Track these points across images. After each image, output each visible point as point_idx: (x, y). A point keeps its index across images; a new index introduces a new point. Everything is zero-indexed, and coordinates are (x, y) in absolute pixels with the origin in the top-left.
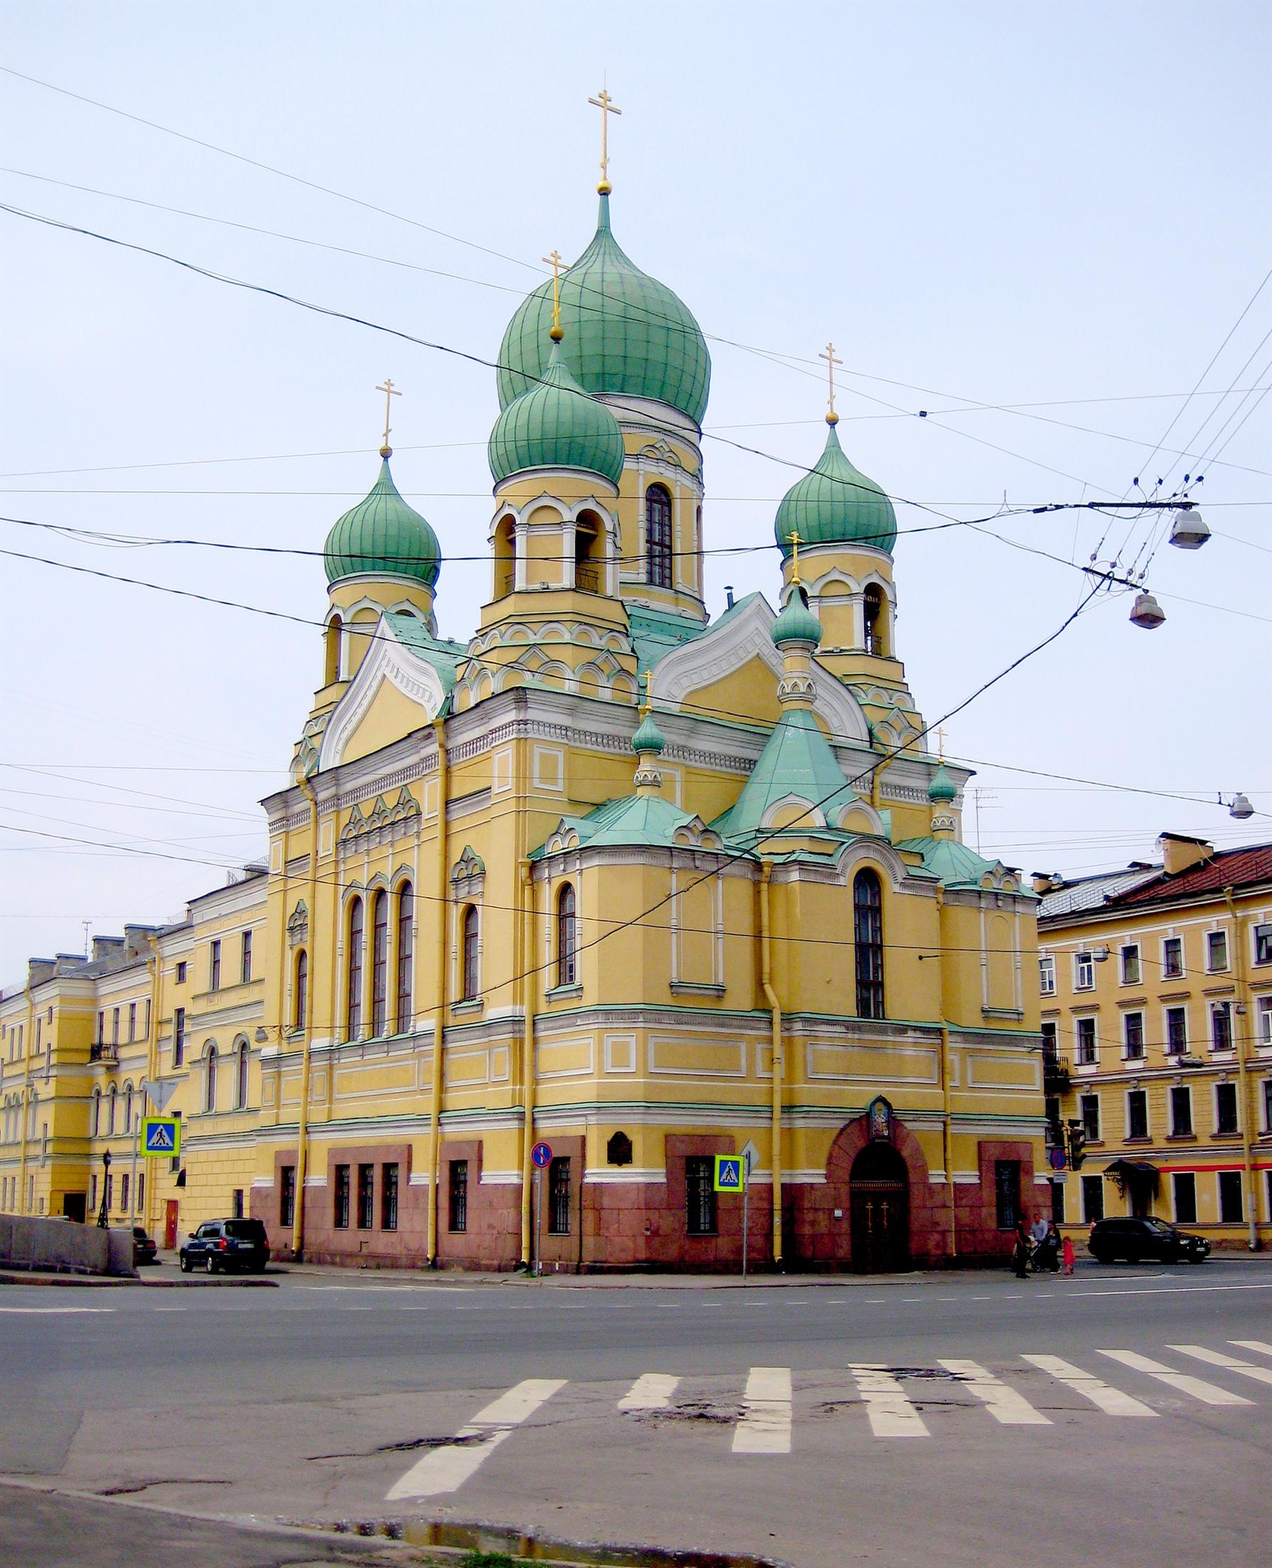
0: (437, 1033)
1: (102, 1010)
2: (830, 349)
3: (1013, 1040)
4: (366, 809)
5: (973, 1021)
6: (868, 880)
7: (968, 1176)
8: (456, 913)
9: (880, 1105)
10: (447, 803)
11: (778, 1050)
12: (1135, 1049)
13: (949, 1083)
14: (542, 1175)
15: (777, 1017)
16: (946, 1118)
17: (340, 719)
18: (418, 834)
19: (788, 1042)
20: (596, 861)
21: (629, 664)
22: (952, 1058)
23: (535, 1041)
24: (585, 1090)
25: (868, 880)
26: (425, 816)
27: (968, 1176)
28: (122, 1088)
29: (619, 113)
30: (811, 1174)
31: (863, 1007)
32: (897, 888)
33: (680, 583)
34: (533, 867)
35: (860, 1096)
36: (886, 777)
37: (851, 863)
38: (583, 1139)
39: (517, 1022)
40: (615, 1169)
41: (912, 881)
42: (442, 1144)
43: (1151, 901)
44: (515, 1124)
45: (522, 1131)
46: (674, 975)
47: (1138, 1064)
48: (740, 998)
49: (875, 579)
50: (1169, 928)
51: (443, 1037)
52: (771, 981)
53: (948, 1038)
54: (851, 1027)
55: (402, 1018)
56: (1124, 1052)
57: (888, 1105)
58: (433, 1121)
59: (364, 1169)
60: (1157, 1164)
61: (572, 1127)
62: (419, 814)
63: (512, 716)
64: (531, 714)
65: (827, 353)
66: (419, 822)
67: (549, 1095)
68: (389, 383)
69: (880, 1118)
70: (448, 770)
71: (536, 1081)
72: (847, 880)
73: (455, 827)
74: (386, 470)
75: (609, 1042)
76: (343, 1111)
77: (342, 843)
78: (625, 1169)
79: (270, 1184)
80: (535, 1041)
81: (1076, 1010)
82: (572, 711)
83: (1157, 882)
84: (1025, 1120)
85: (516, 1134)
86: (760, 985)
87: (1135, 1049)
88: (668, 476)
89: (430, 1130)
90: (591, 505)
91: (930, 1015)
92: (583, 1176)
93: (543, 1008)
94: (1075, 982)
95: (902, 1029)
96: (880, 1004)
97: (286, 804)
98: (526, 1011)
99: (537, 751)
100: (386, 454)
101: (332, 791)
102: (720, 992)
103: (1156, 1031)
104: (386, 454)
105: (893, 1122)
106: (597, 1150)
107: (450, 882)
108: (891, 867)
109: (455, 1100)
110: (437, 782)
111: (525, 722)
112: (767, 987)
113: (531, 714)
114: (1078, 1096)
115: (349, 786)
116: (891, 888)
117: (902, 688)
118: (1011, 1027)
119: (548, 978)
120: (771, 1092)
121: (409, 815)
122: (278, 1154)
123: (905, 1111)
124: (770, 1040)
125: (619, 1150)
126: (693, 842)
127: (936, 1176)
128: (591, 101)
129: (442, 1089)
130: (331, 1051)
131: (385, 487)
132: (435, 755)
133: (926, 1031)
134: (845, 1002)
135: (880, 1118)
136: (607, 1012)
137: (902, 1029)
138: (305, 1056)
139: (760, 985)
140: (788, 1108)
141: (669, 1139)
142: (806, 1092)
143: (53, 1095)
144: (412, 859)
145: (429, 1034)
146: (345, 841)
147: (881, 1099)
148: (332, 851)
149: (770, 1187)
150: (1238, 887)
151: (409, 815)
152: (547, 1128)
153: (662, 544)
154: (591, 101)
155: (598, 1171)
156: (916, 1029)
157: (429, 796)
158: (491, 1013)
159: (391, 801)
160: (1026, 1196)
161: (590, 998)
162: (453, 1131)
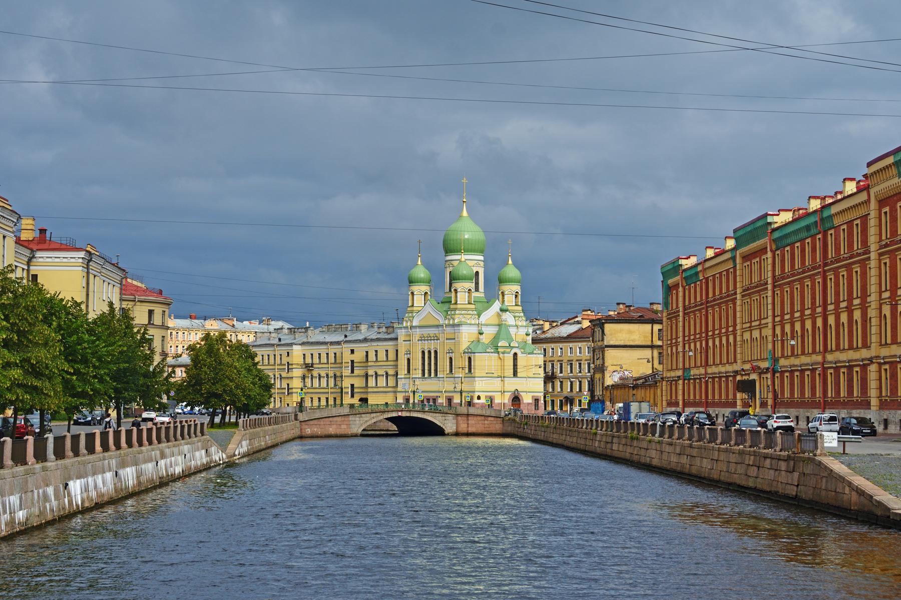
6: (515, 354)
25: (515, 354)
28: (315, 373)
30: (506, 401)
31: (514, 376)
43: (575, 338)
47: (572, 375)
55: (436, 375)
69: (516, 392)
96: (517, 374)
116: (519, 355)
135: (516, 392)
155: (476, 401)
160: (539, 405)
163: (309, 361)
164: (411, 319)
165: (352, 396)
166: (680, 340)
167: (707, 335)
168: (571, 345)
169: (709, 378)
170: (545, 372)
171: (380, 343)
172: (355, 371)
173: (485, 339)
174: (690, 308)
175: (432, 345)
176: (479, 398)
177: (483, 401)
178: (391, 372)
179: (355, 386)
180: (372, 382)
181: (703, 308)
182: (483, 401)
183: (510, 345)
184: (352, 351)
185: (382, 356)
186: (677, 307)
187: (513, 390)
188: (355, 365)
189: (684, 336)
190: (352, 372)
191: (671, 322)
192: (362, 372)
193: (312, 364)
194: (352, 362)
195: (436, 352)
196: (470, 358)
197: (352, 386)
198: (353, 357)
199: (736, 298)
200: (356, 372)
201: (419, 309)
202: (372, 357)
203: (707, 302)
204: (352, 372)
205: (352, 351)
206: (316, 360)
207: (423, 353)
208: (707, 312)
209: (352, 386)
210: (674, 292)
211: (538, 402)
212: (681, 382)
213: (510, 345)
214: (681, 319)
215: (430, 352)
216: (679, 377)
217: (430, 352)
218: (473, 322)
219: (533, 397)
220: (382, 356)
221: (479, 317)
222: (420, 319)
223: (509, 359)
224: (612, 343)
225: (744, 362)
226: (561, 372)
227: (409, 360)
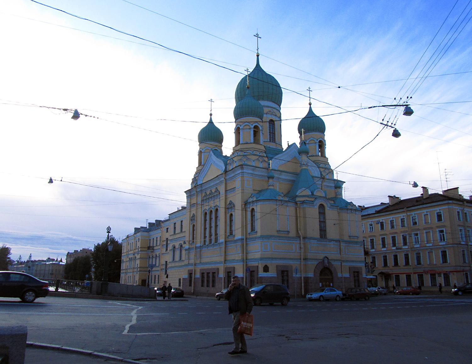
0: (224, 242)
2: (309, 88)
3: (356, 243)
5: (346, 238)
6: (322, 206)
7: (347, 275)
8: (228, 216)
9: (326, 258)
10: (226, 191)
11: (302, 246)
12: (384, 246)
13: (342, 253)
14: (248, 274)
15: (302, 238)
16: (342, 261)
17: (202, 173)
18: (220, 199)
19: (304, 244)
20: (260, 203)
23: (246, 244)
24: (258, 255)
25: (322, 206)
26: (221, 194)
27: (347, 275)
29: (261, 38)
30: (311, 275)
32: (328, 208)
34: (245, 205)
35: (321, 256)
36: (324, 184)
37: (318, 202)
38: (258, 266)
39: (242, 239)
40: (265, 273)
42: (226, 268)
44: (242, 263)
45: (244, 265)
46: (278, 229)
47: (385, 249)
48: (293, 234)
49: (321, 139)
50: (391, 217)
51: (226, 243)
52: (300, 230)
53: (341, 243)
56: (381, 246)
57: (327, 258)
58: (223, 263)
59: (208, 273)
60: (390, 273)
61: (255, 264)
63: (240, 171)
64: (244, 171)
65: (309, 89)
66: (220, 195)
67: (250, 256)
68: (211, 100)
69: (326, 261)
70: (226, 184)
72: (317, 207)
73: (228, 196)
74: (211, 118)
76: (204, 260)
77: (202, 201)
78: (267, 273)
79: (187, 277)
80: (246, 244)
81: (370, 236)
82: (253, 170)
83: (388, 207)
84: (360, 262)
85: (242, 265)
86: (297, 231)
87: (384, 246)
88: (274, 118)
89: (222, 265)
90: (256, 124)
91: (337, 237)
92: (258, 275)
93: (248, 237)
94: (369, 230)
96: (325, 235)
97: (190, 193)
98: (244, 237)
100: (211, 115)
101: (200, 189)
103: (389, 241)
104: (211, 115)
105: (329, 263)
106: (261, 269)
107: (227, 209)
108: (327, 204)
109: (230, 258)
111: (243, 172)
112: (299, 231)
113: (244, 171)
115: (204, 188)
116: (327, 209)
120: (301, 255)
122: (189, 270)
123: (331, 260)
124: (300, 243)
125: (266, 269)
127: (340, 275)
128: (254, 36)
129: (225, 255)
131: (211, 122)
132: (223, 181)
133: (336, 241)
134: (317, 234)
135: (326, 261)
136: (262, 237)
137: (331, 240)
138: (195, 248)
139: (297, 231)
140: (305, 259)
141: (277, 266)
142: (309, 256)
145: (222, 243)
146: (203, 200)
147: (326, 257)
148: (200, 202)
149: (301, 277)
150: (407, 208)
153: (272, 133)
154: (254, 36)
155: (262, 274)
156: (334, 241)
157: (222, 189)
158: (236, 238)
159: (213, 191)
161: (259, 234)
162: (229, 265)
173: (279, 186)
175: (212, 204)
176: (266, 269)
177: (272, 273)
182: (272, 273)
183: (313, 194)
187: (321, 258)
193: (153, 247)
211: (358, 276)
213: (313, 194)
218: (261, 165)
219: (350, 268)
223: (313, 212)
226: (373, 248)
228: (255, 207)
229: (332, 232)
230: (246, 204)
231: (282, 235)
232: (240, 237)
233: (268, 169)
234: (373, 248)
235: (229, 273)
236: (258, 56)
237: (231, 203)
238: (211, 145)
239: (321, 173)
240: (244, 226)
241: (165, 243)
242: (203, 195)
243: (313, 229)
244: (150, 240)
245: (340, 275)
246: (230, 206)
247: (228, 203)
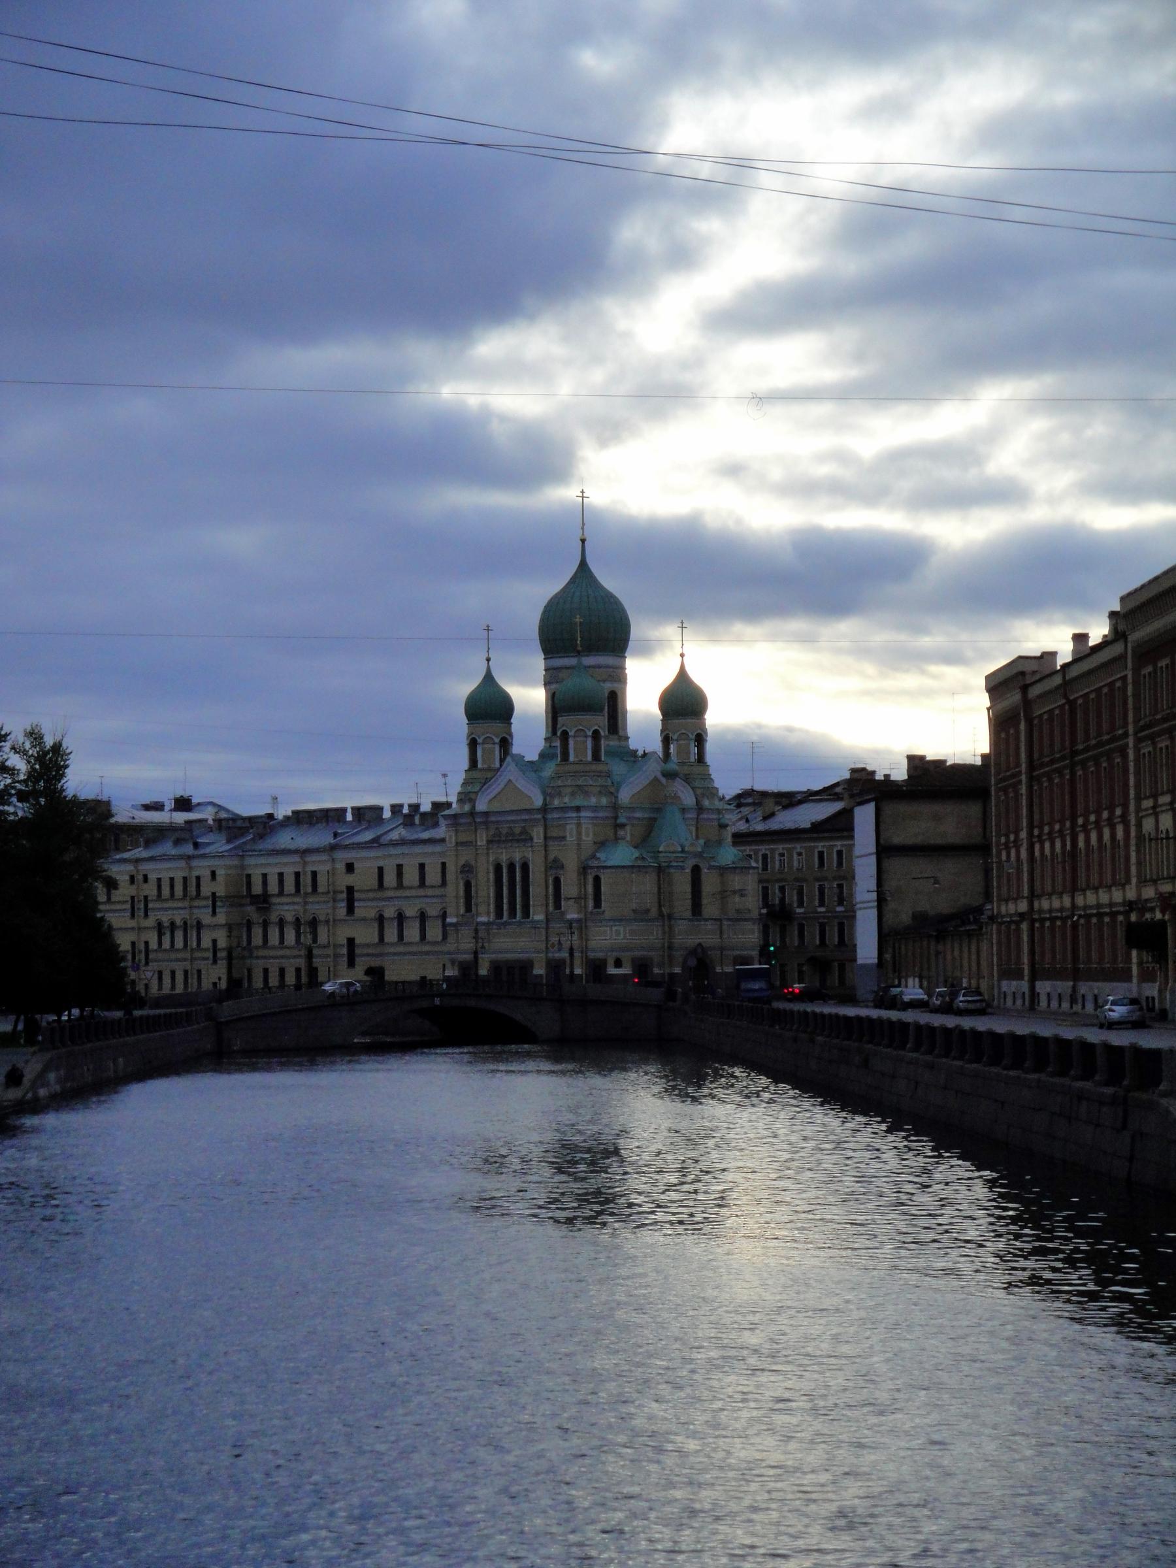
1: (250, 872)
3: (746, 920)
4: (504, 831)
6: (696, 870)
11: (667, 929)
16: (722, 949)
21: (612, 790)
22: (725, 927)
25: (696, 870)
26: (535, 841)
30: (677, 970)
33: (621, 733)
36: (701, 816)
37: (690, 863)
39: (579, 921)
41: (711, 868)
48: (654, 912)
49: (699, 731)
54: (690, 920)
55: (526, 913)
61: (601, 955)
62: (531, 839)
64: (583, 814)
67: (592, 944)
69: (699, 950)
71: (587, 940)
72: (688, 871)
75: (614, 929)
77: (489, 842)
95: (706, 920)
99: (584, 826)
100: (488, 660)
102: (647, 911)
104: (488, 660)
106: (611, 962)
110: (541, 830)
114: (796, 923)
117: (707, 777)
118: (747, 916)
119: (591, 904)
121: (525, 838)
124: (663, 925)
126: (640, 863)
127: (718, 970)
130: (488, 924)
132: (539, 820)
133: (715, 919)
135: (699, 950)
139: (660, 906)
143: (224, 922)
144: (530, 856)
151: (525, 838)
152: (592, 955)
155: (612, 971)
157: (538, 833)
159: (517, 831)
161: (608, 915)
163: (257, 889)
164: (473, 796)
165: (351, 963)
166: (1023, 835)
167: (1074, 824)
168: (820, 846)
169: (1080, 916)
170: (766, 904)
171: (405, 849)
172: (356, 910)
174: (1042, 765)
177: (626, 970)
178: (433, 911)
179: (357, 941)
180: (391, 934)
181: (1065, 767)
184: (350, 868)
185: (410, 877)
186: (1018, 765)
188: (356, 895)
189: (1031, 826)
190: (351, 910)
191: (1006, 794)
192: (372, 913)
194: (350, 890)
195: (525, 867)
196: (597, 880)
197: (351, 941)
198: (350, 880)
199: (1127, 745)
200: (359, 912)
201: (489, 775)
202: (390, 879)
203: (1074, 753)
204: (351, 910)
205: (350, 868)
206: (273, 888)
207: (498, 868)
208: (1073, 774)
209: (351, 941)
210: (1012, 731)
212: (1024, 926)
214: (1023, 790)
215: (512, 866)
216: (1022, 915)
217: (512, 866)
220: (410, 877)
221: (618, 791)
222: (492, 795)
224: (897, 840)
225: (1143, 882)
226: (801, 904)
227: (468, 885)
228: (602, 877)
229: (710, 908)
230: (584, 870)
231: (641, 915)
232: (575, 916)
233: (615, 807)
234: (801, 904)
235: (555, 967)
236: (583, 541)
237: (556, 860)
238: (493, 729)
239: (696, 795)
240: (580, 899)
241: (344, 895)
242: (492, 832)
243: (683, 906)
244: (249, 876)
245: (718, 970)
246: (555, 866)
247: (551, 857)
